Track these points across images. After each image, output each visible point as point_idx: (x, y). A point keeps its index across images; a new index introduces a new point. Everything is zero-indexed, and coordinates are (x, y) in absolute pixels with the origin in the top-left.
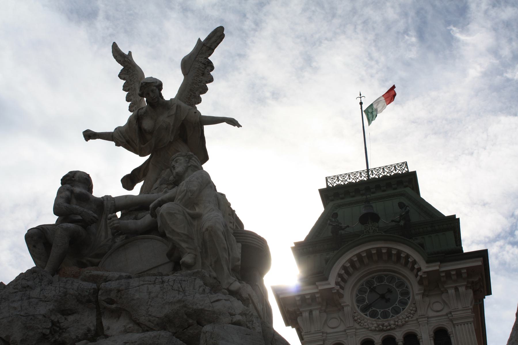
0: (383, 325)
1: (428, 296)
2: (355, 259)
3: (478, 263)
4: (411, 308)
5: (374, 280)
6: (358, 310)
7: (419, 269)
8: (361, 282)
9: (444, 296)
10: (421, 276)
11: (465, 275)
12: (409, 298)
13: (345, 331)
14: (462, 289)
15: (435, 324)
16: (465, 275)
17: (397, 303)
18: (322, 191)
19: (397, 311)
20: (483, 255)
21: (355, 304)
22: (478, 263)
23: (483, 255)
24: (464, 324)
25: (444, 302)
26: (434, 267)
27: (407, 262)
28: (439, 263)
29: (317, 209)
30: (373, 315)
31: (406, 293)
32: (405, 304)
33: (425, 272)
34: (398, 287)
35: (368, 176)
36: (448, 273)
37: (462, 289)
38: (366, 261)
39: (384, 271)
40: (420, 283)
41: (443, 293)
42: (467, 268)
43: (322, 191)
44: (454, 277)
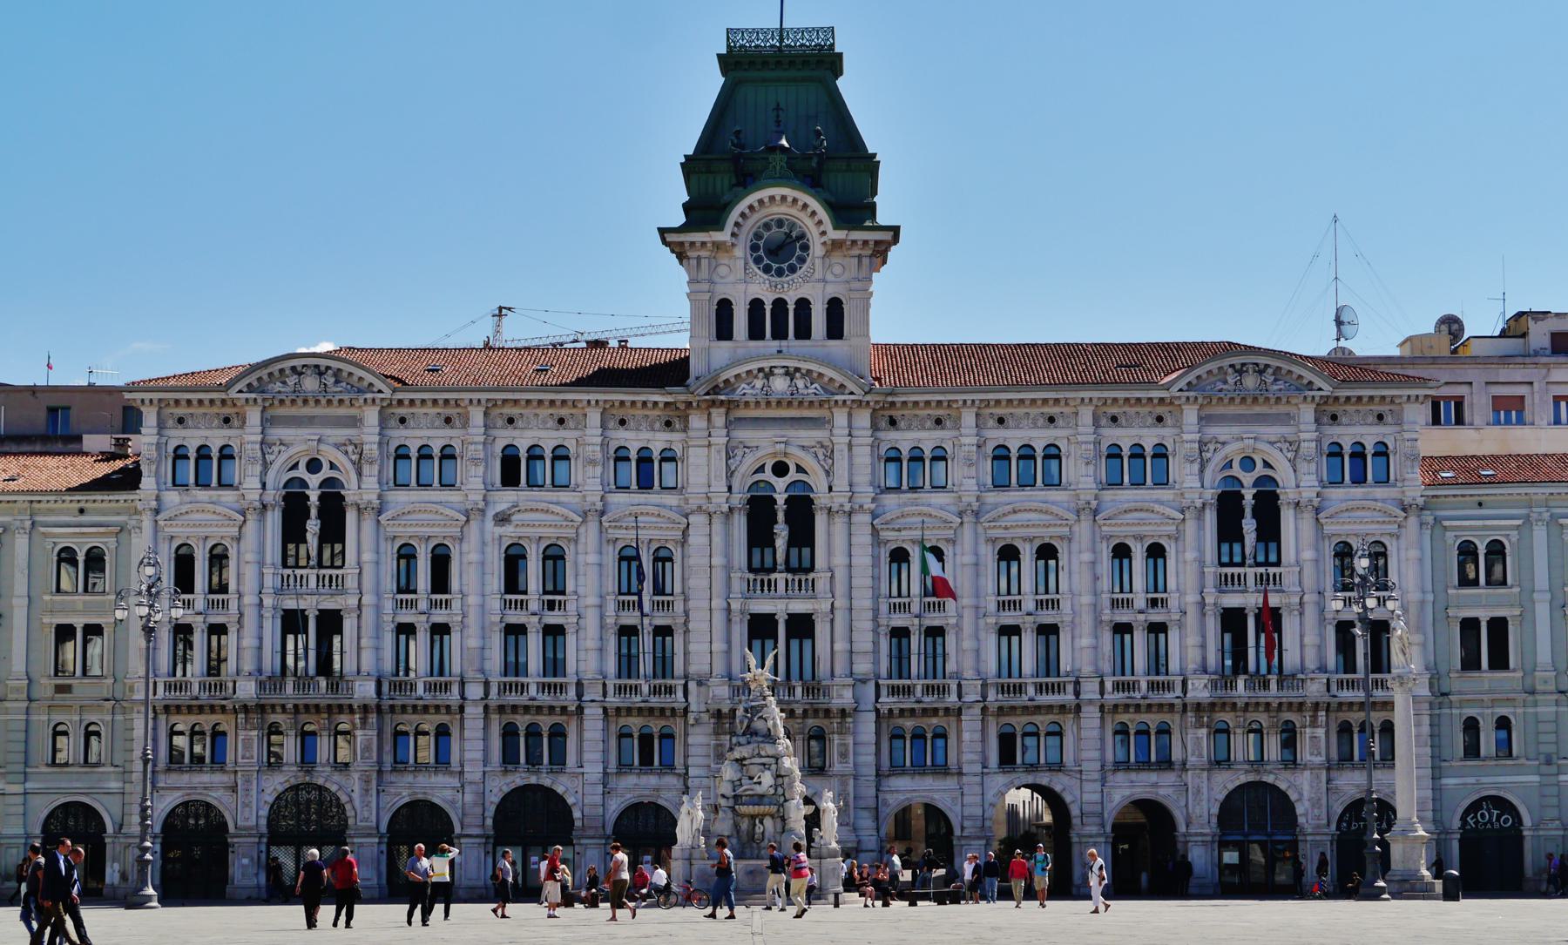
3: (888, 236)
6: (751, 262)
7: (824, 233)
14: (866, 261)
15: (833, 291)
18: (719, 56)
19: (793, 270)
20: (895, 230)
22: (888, 236)
23: (895, 230)
26: (840, 235)
29: (715, 81)
30: (767, 270)
31: (805, 248)
35: (781, 40)
36: (854, 242)
43: (719, 56)
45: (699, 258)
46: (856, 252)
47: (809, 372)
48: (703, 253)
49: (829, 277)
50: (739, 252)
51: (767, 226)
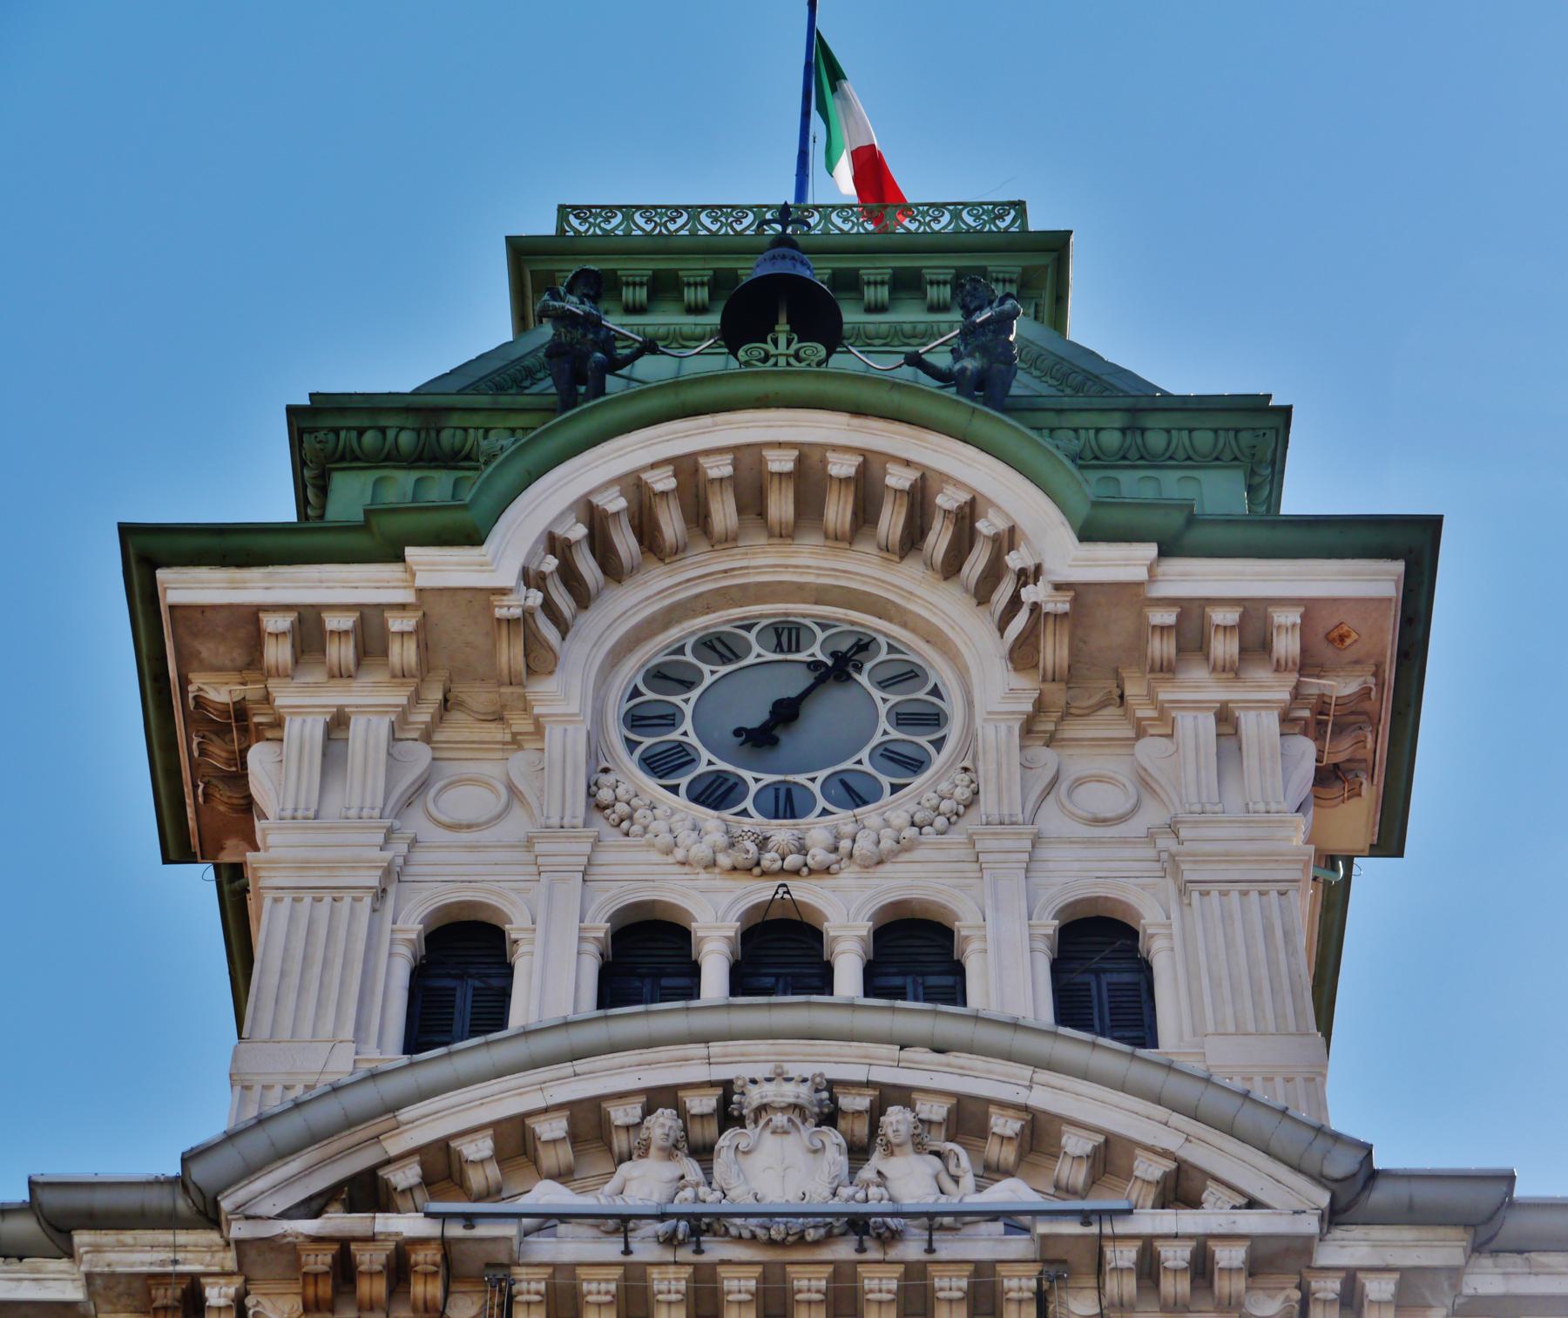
0: (763, 843)
1: (1051, 741)
2: (663, 481)
3: (1378, 580)
4: (944, 786)
5: (751, 637)
8: (674, 633)
9: (1150, 750)
10: (1035, 607)
11: (1287, 645)
12: (939, 744)
13: (529, 843)
14: (1260, 727)
15: (1080, 874)
16: (1287, 645)
17: (864, 754)
19: (853, 794)
20: (1413, 543)
21: (616, 733)
23: (1413, 543)
24: (1245, 893)
25: (1145, 782)
27: (961, 544)
28: (1151, 550)
30: (716, 793)
32: (915, 765)
33: (1058, 587)
34: (884, 685)
36: (1192, 612)
37: (1260, 727)
38: (723, 512)
39: (821, 595)
40: (1023, 655)
41: (1140, 733)
42: (1310, 607)
43: (521, 251)
44: (1224, 648)
45: (338, 723)
46: (1200, 686)
47: (967, 1120)
48: (373, 700)
49: (1052, 820)
50: (574, 697)
51: (718, 647)
